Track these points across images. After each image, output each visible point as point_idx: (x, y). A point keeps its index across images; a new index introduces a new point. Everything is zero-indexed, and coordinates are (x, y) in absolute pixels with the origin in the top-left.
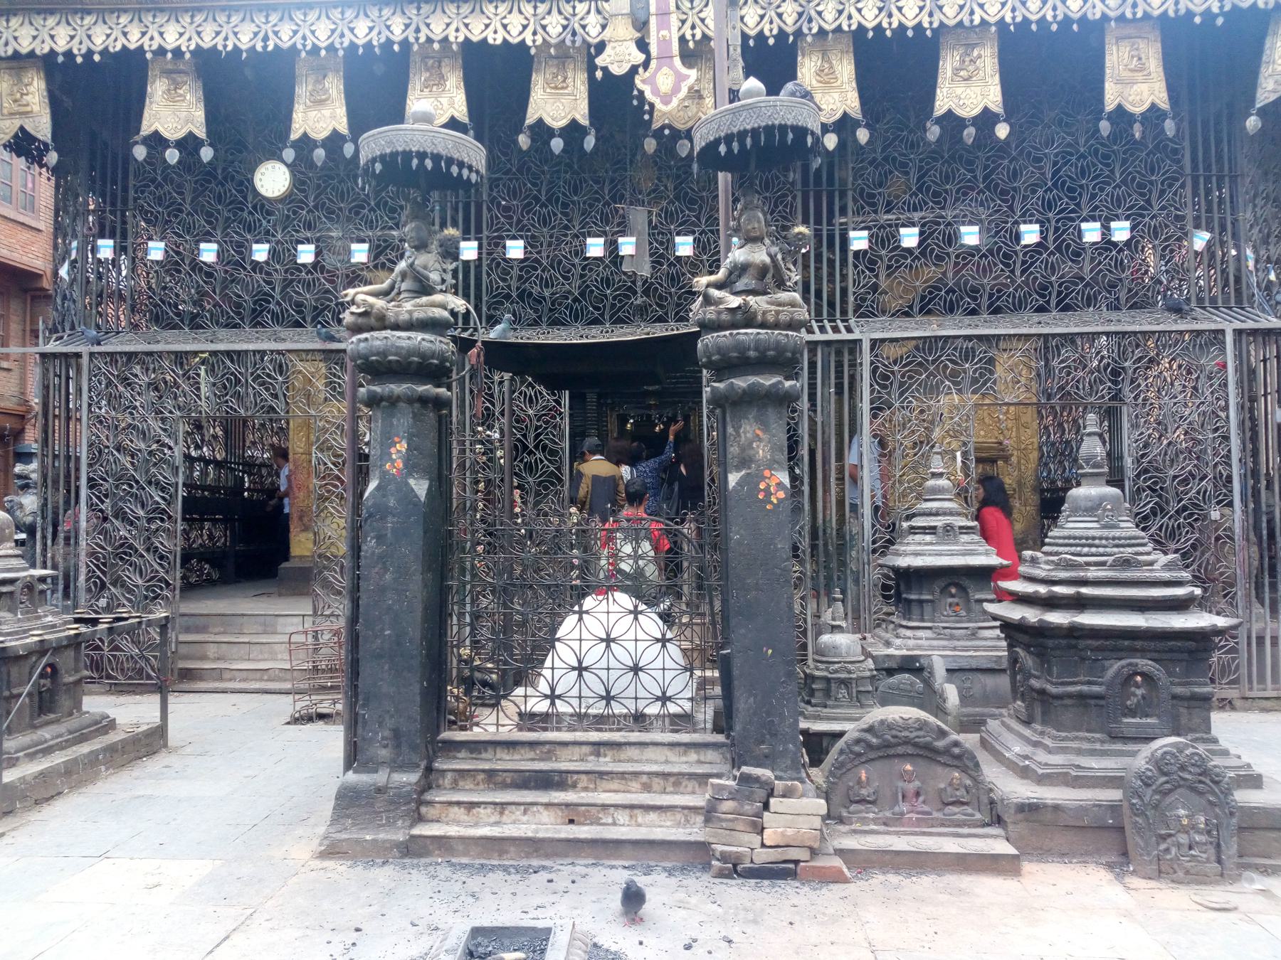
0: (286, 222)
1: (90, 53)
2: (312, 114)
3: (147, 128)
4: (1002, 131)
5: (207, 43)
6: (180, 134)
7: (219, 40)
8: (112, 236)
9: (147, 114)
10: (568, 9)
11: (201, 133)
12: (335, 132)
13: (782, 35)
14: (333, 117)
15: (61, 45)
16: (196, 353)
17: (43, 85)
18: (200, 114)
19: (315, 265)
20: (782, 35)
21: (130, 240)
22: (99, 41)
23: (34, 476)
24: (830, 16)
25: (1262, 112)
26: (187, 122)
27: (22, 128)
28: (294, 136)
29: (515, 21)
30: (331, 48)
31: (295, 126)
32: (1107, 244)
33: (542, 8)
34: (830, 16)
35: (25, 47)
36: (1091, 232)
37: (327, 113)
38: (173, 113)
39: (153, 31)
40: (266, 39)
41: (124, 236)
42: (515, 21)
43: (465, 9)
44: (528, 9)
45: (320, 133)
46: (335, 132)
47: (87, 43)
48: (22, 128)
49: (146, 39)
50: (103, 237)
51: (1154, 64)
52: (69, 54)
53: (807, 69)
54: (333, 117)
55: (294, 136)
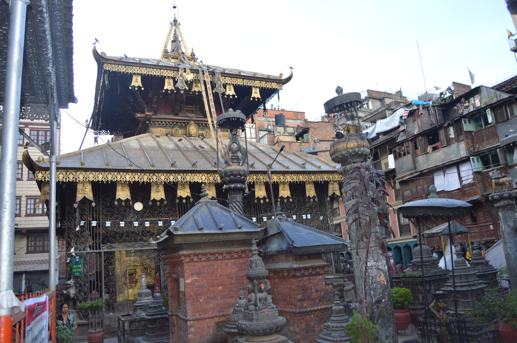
0: (142, 217)
1: (108, 181)
2: (156, 194)
3: (117, 198)
4: (291, 200)
5: (137, 180)
6: (125, 199)
7: (139, 179)
8: (96, 220)
9: (117, 194)
10: (214, 176)
11: (130, 198)
12: (162, 199)
13: (254, 182)
14: (161, 195)
15: (100, 179)
16: (131, 251)
17: (91, 187)
18: (129, 194)
19: (149, 227)
20: (254, 182)
21: (101, 221)
22: (110, 178)
23: (72, 284)
24: (262, 179)
25: (329, 197)
26: (127, 195)
27: (85, 197)
28: (152, 199)
29: (203, 177)
30: (165, 182)
31: (151, 197)
32: (307, 219)
33: (209, 175)
34: (262, 179)
35: (91, 179)
36: (304, 217)
37: (159, 194)
38: (123, 194)
39: (123, 177)
40: (150, 179)
41: (99, 220)
42: (203, 177)
43: (193, 175)
44: (206, 175)
45: (158, 198)
46: (162, 199)
47: (106, 179)
48: (85, 197)
49: (122, 179)
50: (93, 220)
51: (313, 189)
52: (102, 181)
53: (257, 188)
54: (161, 195)
55: (152, 199)
